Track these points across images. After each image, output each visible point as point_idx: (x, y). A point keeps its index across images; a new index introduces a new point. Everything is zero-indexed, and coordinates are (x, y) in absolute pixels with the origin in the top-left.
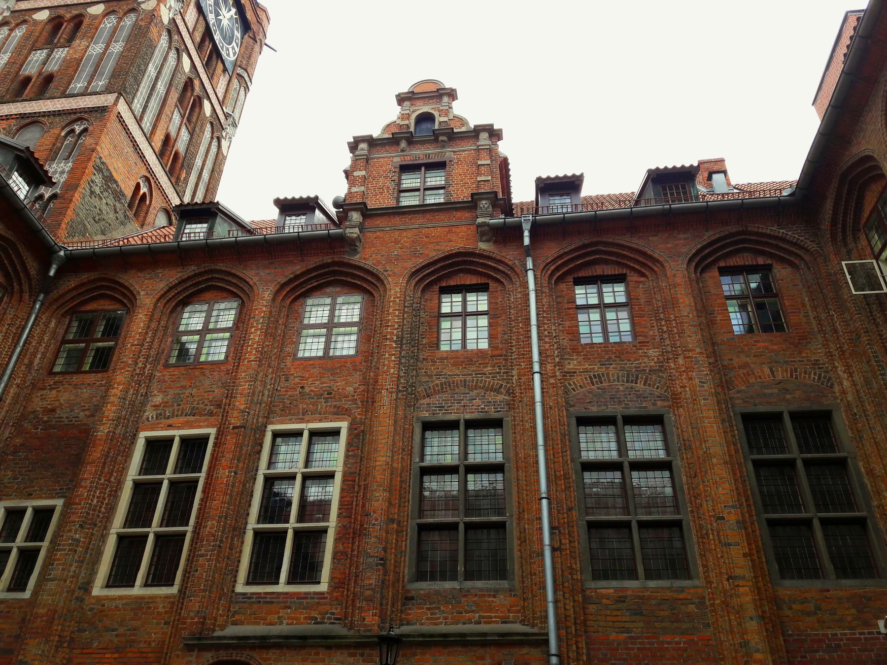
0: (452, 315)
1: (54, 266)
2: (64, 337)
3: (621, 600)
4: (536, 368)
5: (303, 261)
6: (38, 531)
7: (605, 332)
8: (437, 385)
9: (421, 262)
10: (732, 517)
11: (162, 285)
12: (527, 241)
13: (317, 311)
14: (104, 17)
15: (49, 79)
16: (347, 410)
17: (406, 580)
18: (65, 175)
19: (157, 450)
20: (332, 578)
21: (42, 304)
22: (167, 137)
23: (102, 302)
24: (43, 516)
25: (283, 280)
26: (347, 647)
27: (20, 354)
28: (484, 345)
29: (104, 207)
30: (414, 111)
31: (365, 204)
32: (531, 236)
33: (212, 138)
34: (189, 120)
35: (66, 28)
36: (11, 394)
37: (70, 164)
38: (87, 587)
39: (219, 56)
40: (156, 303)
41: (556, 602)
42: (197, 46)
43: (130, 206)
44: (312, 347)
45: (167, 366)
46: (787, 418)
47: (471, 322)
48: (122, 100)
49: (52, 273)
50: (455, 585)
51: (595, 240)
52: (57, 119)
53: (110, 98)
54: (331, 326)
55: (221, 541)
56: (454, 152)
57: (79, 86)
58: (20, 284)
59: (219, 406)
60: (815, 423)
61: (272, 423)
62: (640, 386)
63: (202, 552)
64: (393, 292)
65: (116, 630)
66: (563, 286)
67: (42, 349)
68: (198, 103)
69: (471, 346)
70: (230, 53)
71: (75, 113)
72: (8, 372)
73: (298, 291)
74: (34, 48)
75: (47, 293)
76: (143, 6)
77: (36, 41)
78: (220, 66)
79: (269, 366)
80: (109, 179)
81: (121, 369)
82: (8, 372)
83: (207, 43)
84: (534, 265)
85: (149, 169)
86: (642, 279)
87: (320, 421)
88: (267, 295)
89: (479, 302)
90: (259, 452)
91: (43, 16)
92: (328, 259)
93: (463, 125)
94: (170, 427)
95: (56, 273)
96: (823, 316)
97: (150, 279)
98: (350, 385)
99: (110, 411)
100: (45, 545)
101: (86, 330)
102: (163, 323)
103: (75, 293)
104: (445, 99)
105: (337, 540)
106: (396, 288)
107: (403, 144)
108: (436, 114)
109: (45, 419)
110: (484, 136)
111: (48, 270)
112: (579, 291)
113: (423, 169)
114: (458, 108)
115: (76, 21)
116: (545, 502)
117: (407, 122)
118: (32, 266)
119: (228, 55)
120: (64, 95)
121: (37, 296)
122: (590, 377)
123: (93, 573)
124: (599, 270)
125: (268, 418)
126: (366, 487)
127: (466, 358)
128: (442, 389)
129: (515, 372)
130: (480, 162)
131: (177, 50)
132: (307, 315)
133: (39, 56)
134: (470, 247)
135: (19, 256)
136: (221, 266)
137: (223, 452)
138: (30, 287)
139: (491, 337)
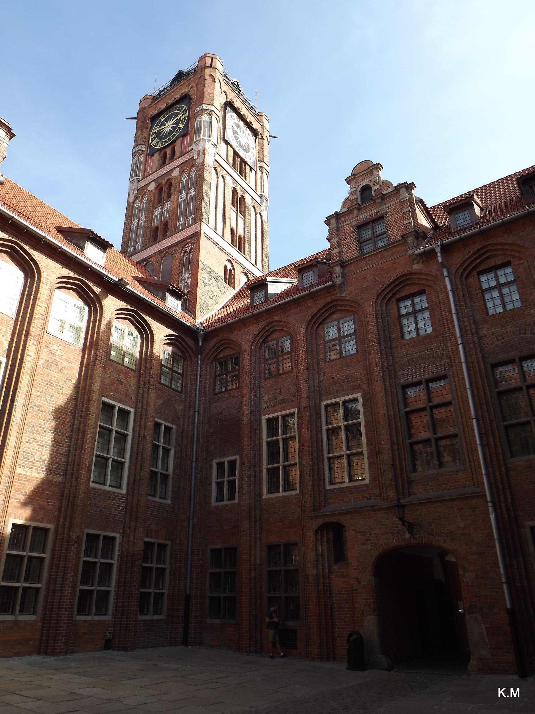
0: (407, 315)
1: (200, 340)
2: (215, 374)
5: (316, 304)
6: (232, 472)
7: (504, 304)
8: (406, 362)
9: (380, 288)
11: (251, 337)
12: (440, 259)
14: (181, 176)
15: (166, 224)
16: (359, 386)
18: (190, 279)
19: (272, 423)
21: (201, 360)
22: (232, 230)
23: (226, 351)
24: (232, 463)
27: (199, 388)
28: (430, 330)
29: (213, 289)
30: (358, 187)
31: (342, 261)
33: (256, 215)
34: (241, 213)
35: (165, 189)
36: (202, 409)
37: (190, 272)
38: (260, 494)
39: (246, 163)
40: (251, 347)
41: (488, 474)
42: (231, 165)
43: (225, 281)
45: (265, 379)
48: (203, 225)
49: (200, 344)
51: (485, 244)
52: (177, 248)
53: (198, 225)
55: (313, 466)
56: (388, 207)
57: (181, 223)
58: (189, 354)
59: (295, 396)
61: (323, 401)
62: (528, 335)
63: (305, 473)
65: (277, 513)
66: (471, 280)
67: (208, 382)
68: (243, 199)
69: (422, 333)
70: (250, 157)
71: (184, 241)
72: (197, 398)
73: (318, 321)
74: (154, 208)
75: (201, 354)
76: (198, 161)
77: (154, 203)
78: (248, 168)
79: (313, 370)
80: (211, 271)
81: (245, 386)
82: (197, 398)
83: (237, 159)
84: (448, 272)
85: (229, 255)
86: (522, 261)
87: (347, 395)
88: (303, 330)
90: (320, 418)
91: (152, 187)
92: (329, 300)
93: (389, 187)
94: (275, 411)
95: (202, 344)
97: (245, 334)
99: (246, 409)
100: (237, 477)
101: (224, 365)
102: (257, 357)
103: (213, 350)
104: (375, 172)
105: (369, 457)
107: (356, 212)
108: (371, 184)
109: (219, 417)
110: (403, 191)
111: (198, 343)
112: (483, 278)
113: (371, 224)
114: (384, 175)
115: (168, 183)
116: (474, 421)
117: (355, 197)
118: (191, 342)
119: (250, 159)
120: (176, 232)
121: (198, 357)
122: (496, 337)
123: (261, 488)
124: (492, 263)
125: (320, 398)
128: (409, 363)
129: (449, 345)
130: (403, 211)
131: (222, 176)
132: (326, 335)
133: (158, 211)
135: (184, 341)
136: (276, 318)
137: (302, 421)
138: (194, 354)
139: (432, 324)
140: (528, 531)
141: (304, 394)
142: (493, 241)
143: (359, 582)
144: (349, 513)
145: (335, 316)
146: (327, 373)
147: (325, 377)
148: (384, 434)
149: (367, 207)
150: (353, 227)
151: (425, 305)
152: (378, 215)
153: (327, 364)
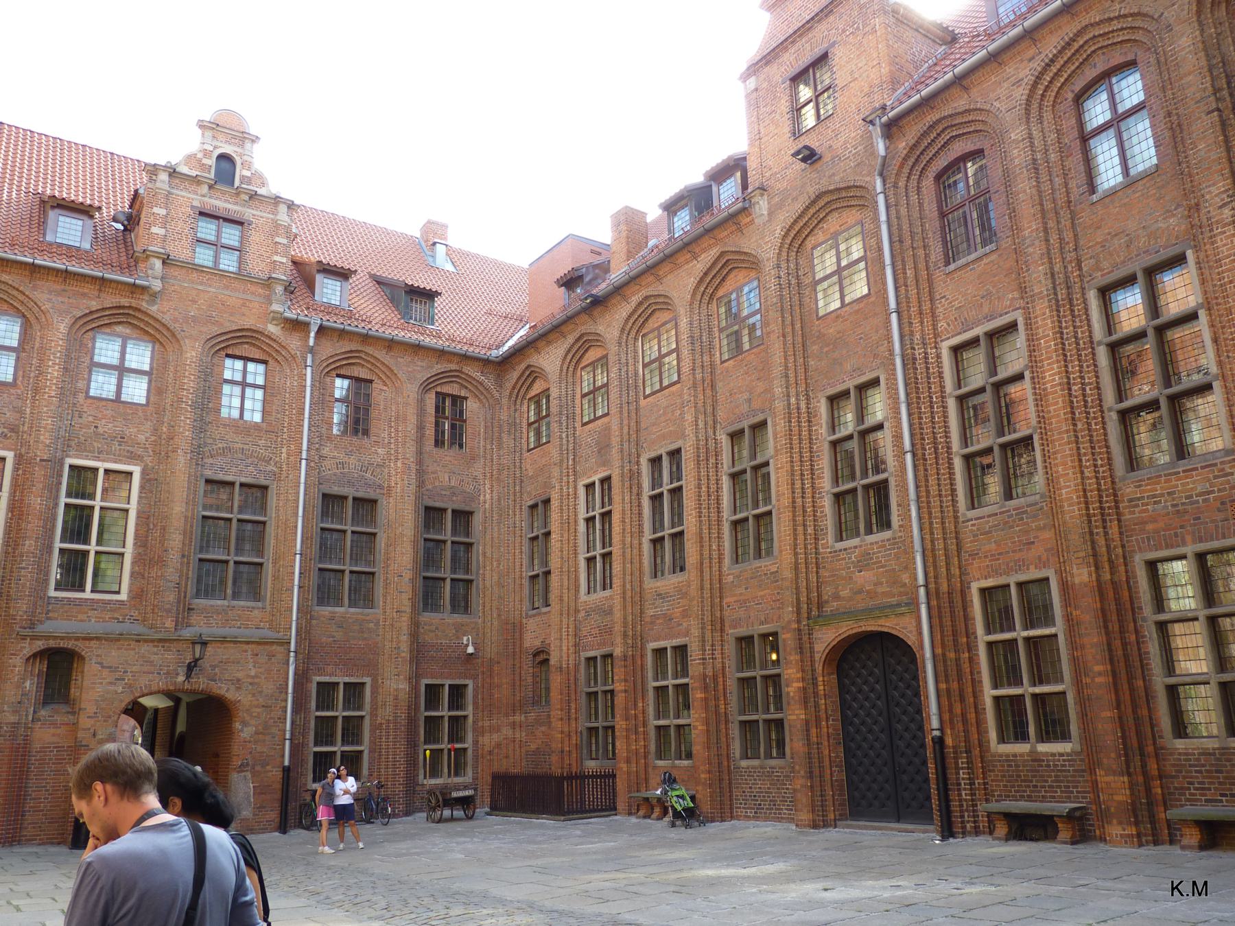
3: (332, 619)
4: (304, 455)
9: (216, 330)
10: (408, 575)
13: (106, 349)
17: (188, 595)
20: (130, 591)
25: (80, 314)
26: (152, 641)
30: (215, 147)
32: (316, 338)
44: (103, 385)
46: (449, 512)
47: (249, 391)
50: (226, 603)
54: (122, 370)
60: (463, 517)
62: (368, 475)
63: (23, 565)
64: (189, 355)
66: (328, 379)
89: (256, 373)
92: (125, 302)
96: (489, 447)
98: (142, 434)
104: (248, 145)
105: (133, 563)
106: (192, 352)
110: (283, 208)
116: (298, 557)
126: (164, 528)
127: (240, 426)
129: (284, 450)
130: (277, 239)
134: (260, 326)
139: (264, 411)
140: (314, 685)
141: (45, 438)
142: (370, 350)
143: (94, 735)
144: (97, 638)
145: (119, 329)
146: (85, 415)
147: (80, 421)
148: (175, 540)
149: (224, 193)
150: (192, 207)
151: (260, 381)
152: (236, 217)
153: (89, 401)
